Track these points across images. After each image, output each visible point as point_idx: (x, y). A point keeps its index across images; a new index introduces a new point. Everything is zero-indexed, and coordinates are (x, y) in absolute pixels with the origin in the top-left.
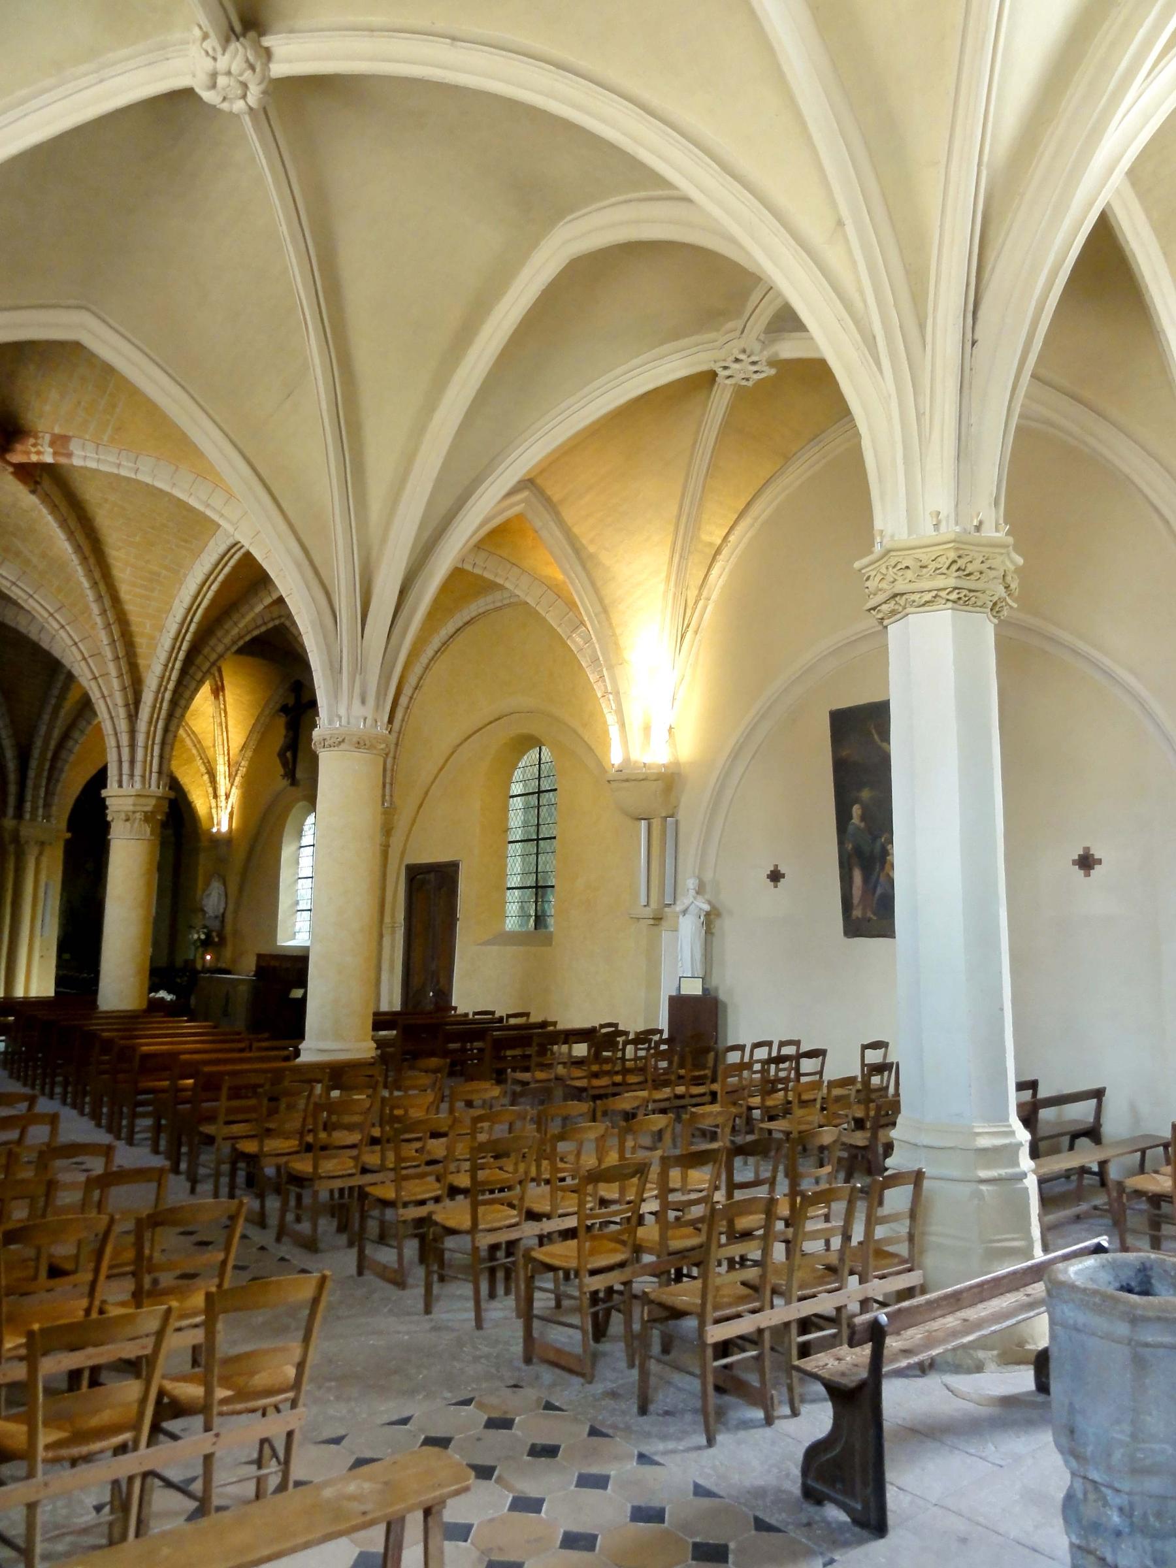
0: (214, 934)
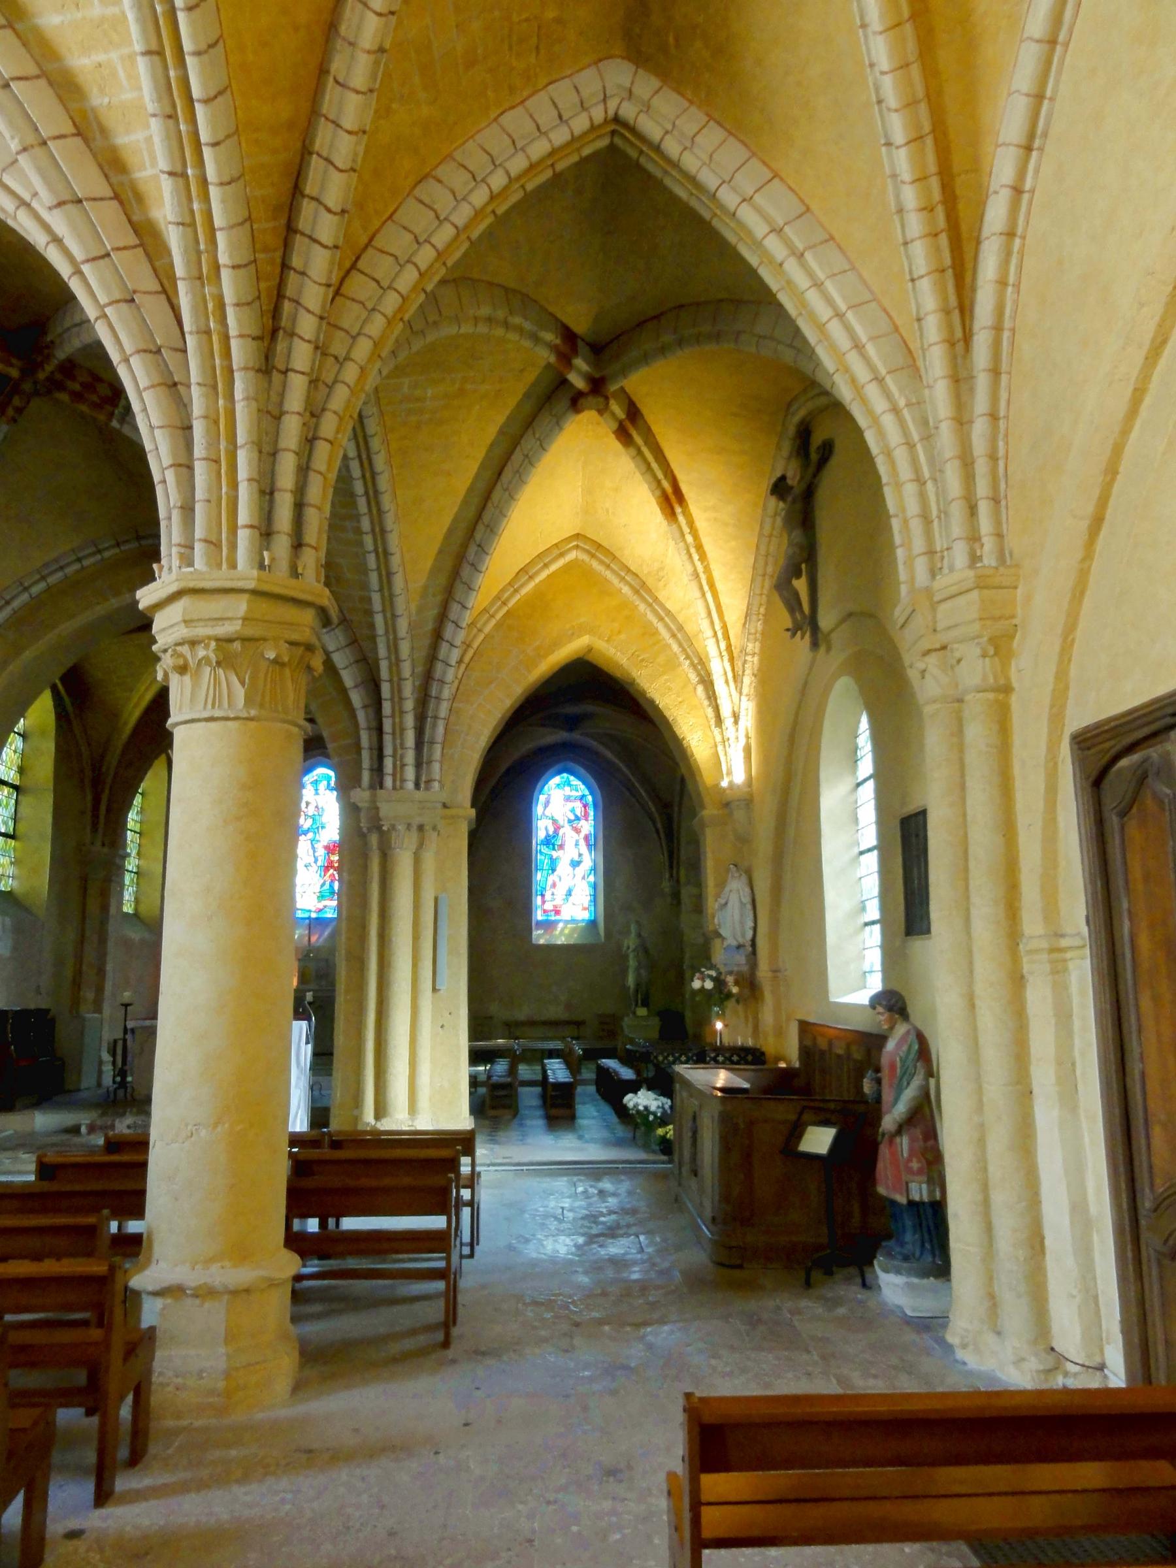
0: (730, 979)
